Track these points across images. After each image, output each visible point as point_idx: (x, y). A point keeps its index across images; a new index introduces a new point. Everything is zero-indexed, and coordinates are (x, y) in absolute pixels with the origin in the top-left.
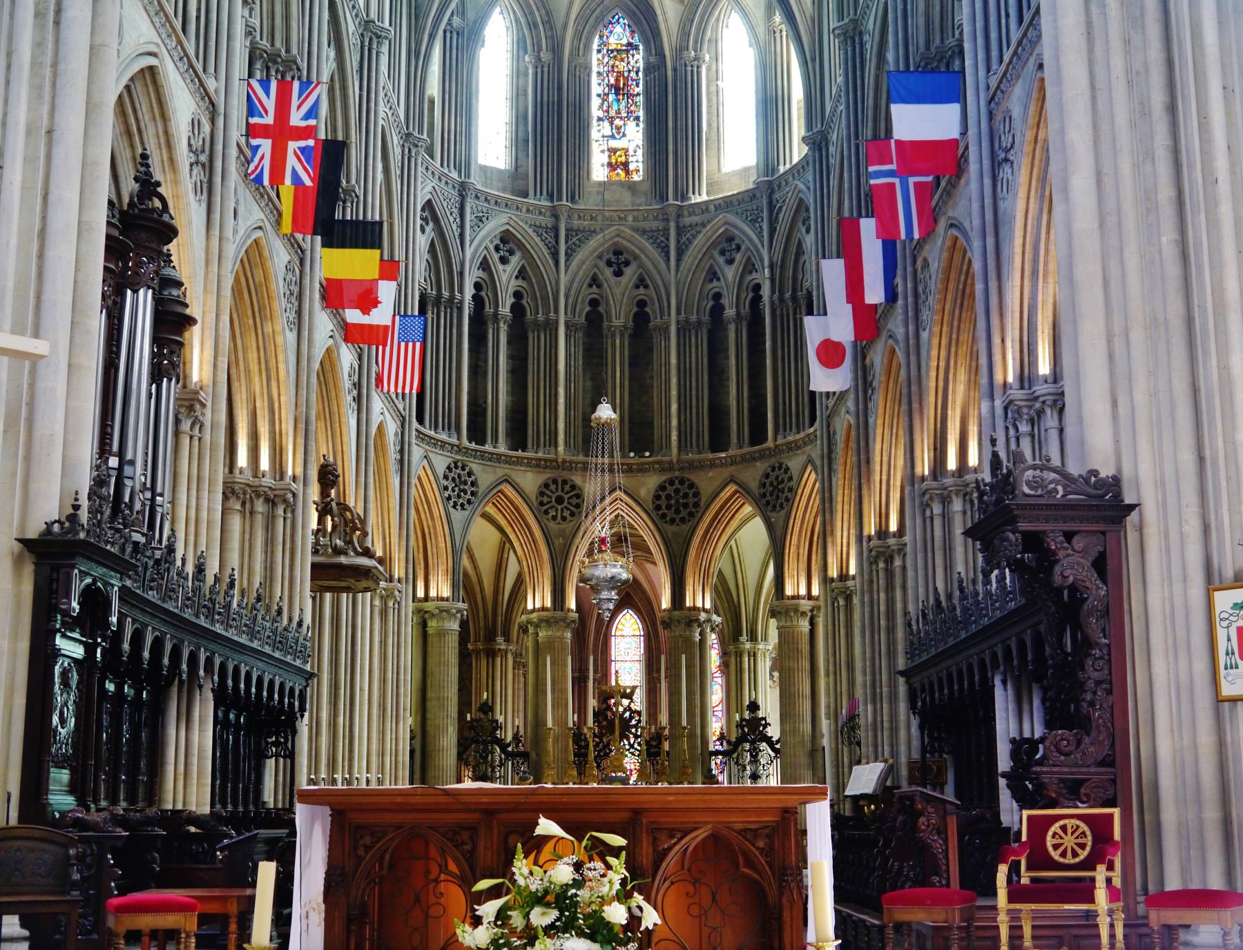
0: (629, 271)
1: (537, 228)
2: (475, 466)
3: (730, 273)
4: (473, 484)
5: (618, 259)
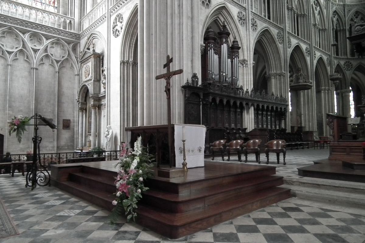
2: (352, 62)
4: (351, 65)
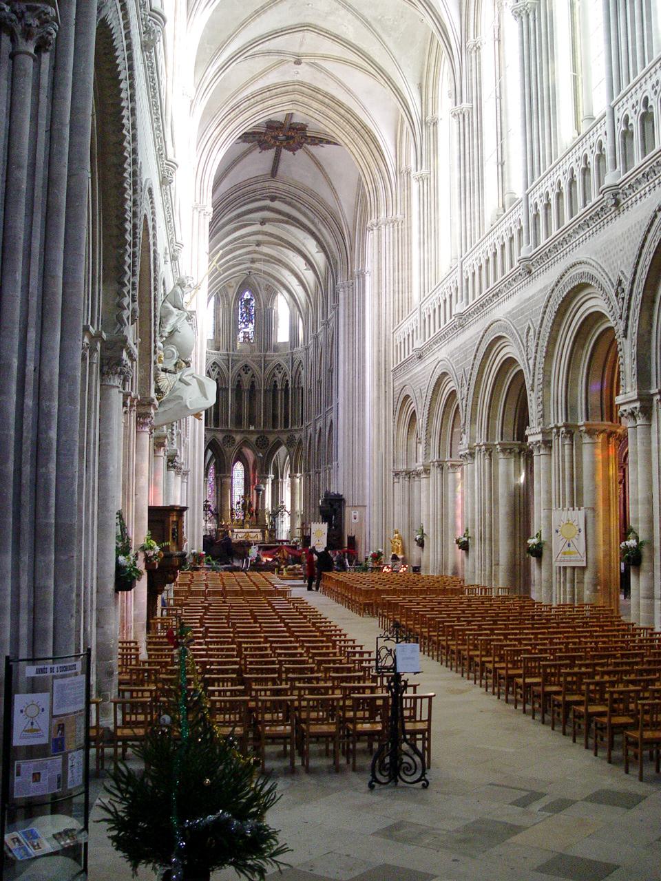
0: (249, 372)
1: (223, 360)
3: (280, 376)
5: (246, 368)
